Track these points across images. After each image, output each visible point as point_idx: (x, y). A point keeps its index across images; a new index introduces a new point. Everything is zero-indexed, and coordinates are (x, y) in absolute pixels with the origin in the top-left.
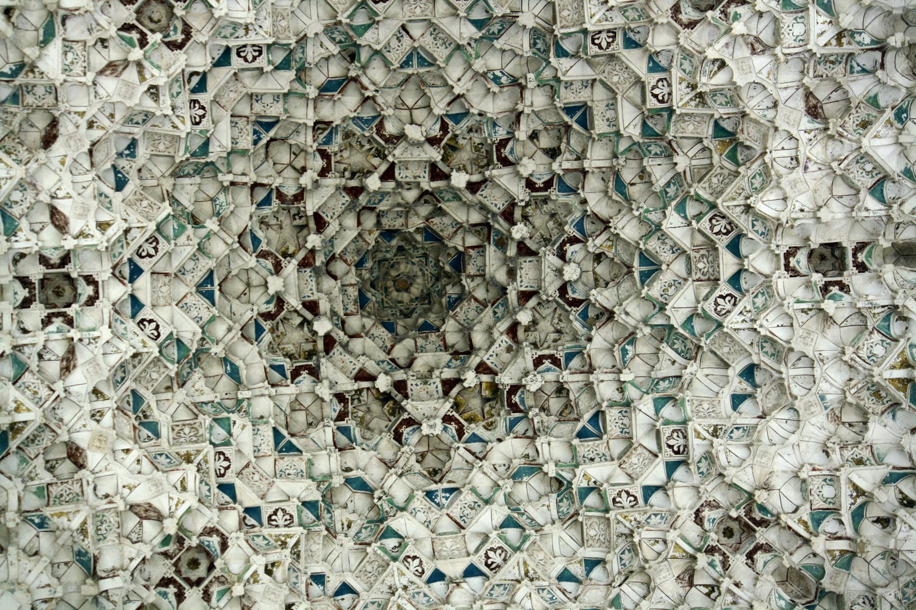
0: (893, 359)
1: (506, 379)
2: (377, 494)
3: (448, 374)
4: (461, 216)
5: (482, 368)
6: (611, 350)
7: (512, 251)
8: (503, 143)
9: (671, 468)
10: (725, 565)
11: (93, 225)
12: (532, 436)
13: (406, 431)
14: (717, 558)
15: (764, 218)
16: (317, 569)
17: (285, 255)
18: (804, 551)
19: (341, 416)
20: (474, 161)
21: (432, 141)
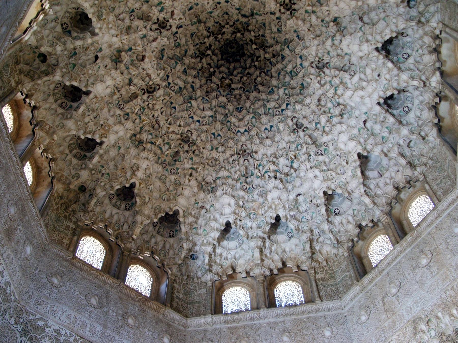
0: (294, 153)
1: (233, 86)
2: (194, 92)
3: (225, 76)
4: (250, 50)
5: (231, 80)
6: (254, 98)
7: (253, 64)
8: (267, 47)
9: (246, 131)
10: (239, 158)
11: (178, 18)
12: (229, 101)
13: (209, 81)
14: (239, 156)
15: (295, 108)
16: (172, 101)
17: (213, 34)
18: (253, 169)
19: (200, 70)
20: (260, 44)
21: (255, 36)
